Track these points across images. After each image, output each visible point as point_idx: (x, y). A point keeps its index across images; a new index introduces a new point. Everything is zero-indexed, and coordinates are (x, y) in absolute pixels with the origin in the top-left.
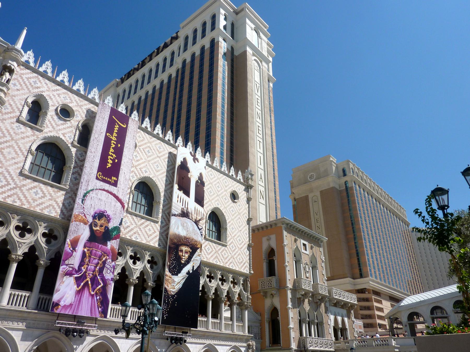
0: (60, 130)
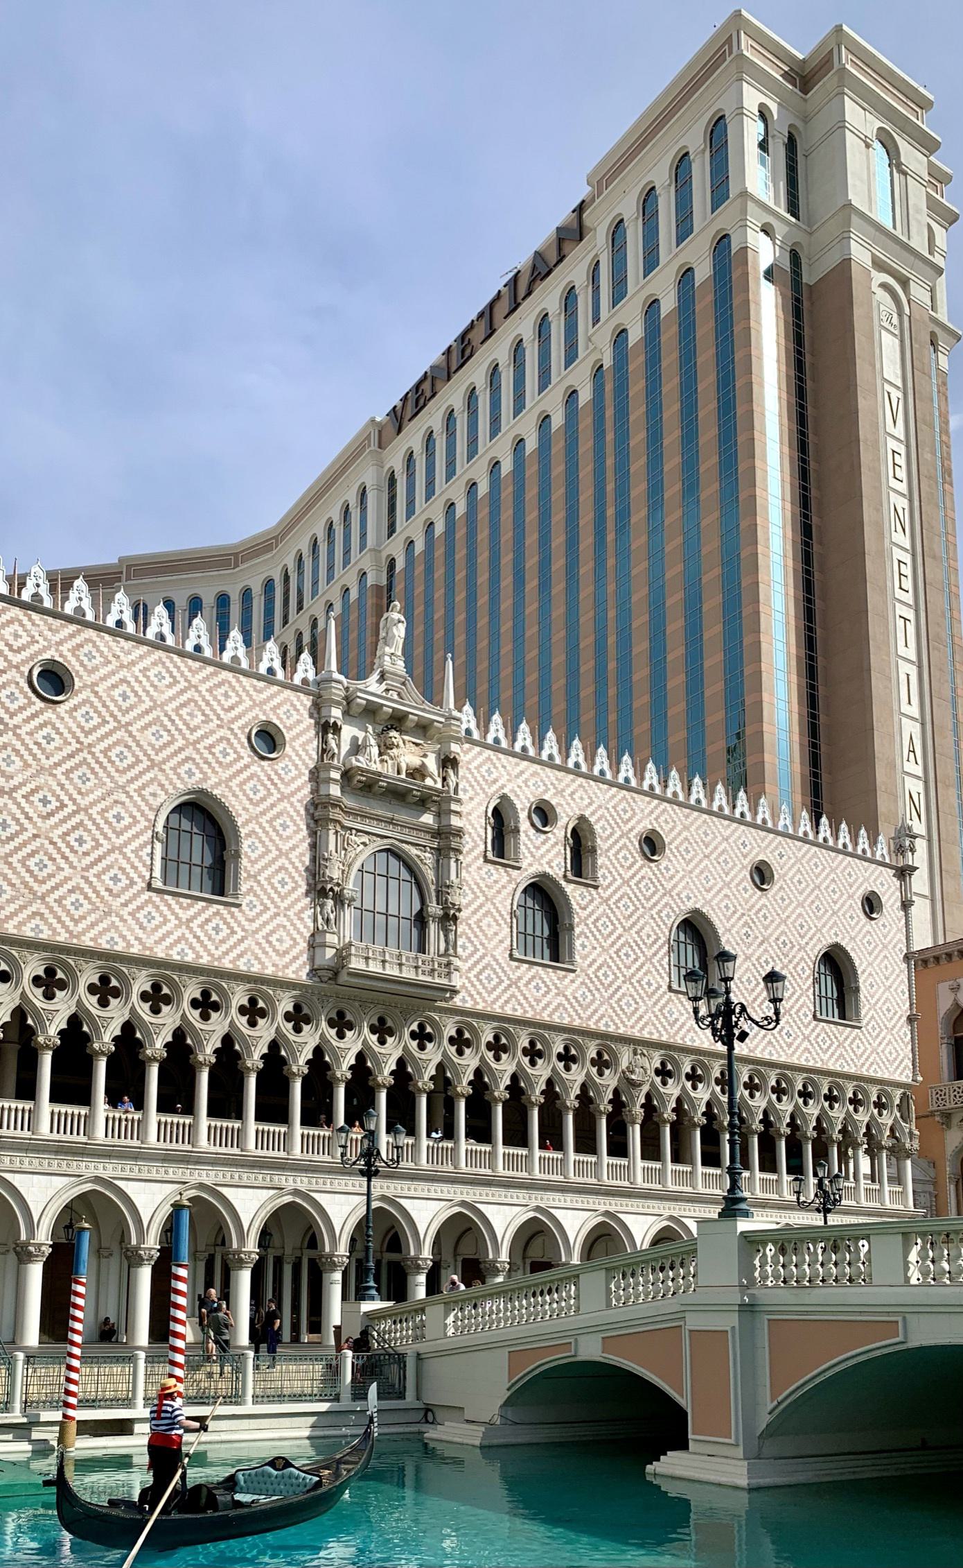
0: (542, 856)
